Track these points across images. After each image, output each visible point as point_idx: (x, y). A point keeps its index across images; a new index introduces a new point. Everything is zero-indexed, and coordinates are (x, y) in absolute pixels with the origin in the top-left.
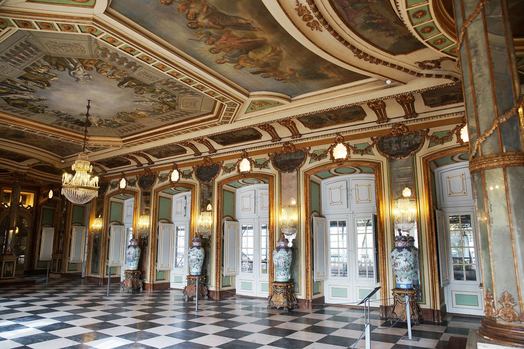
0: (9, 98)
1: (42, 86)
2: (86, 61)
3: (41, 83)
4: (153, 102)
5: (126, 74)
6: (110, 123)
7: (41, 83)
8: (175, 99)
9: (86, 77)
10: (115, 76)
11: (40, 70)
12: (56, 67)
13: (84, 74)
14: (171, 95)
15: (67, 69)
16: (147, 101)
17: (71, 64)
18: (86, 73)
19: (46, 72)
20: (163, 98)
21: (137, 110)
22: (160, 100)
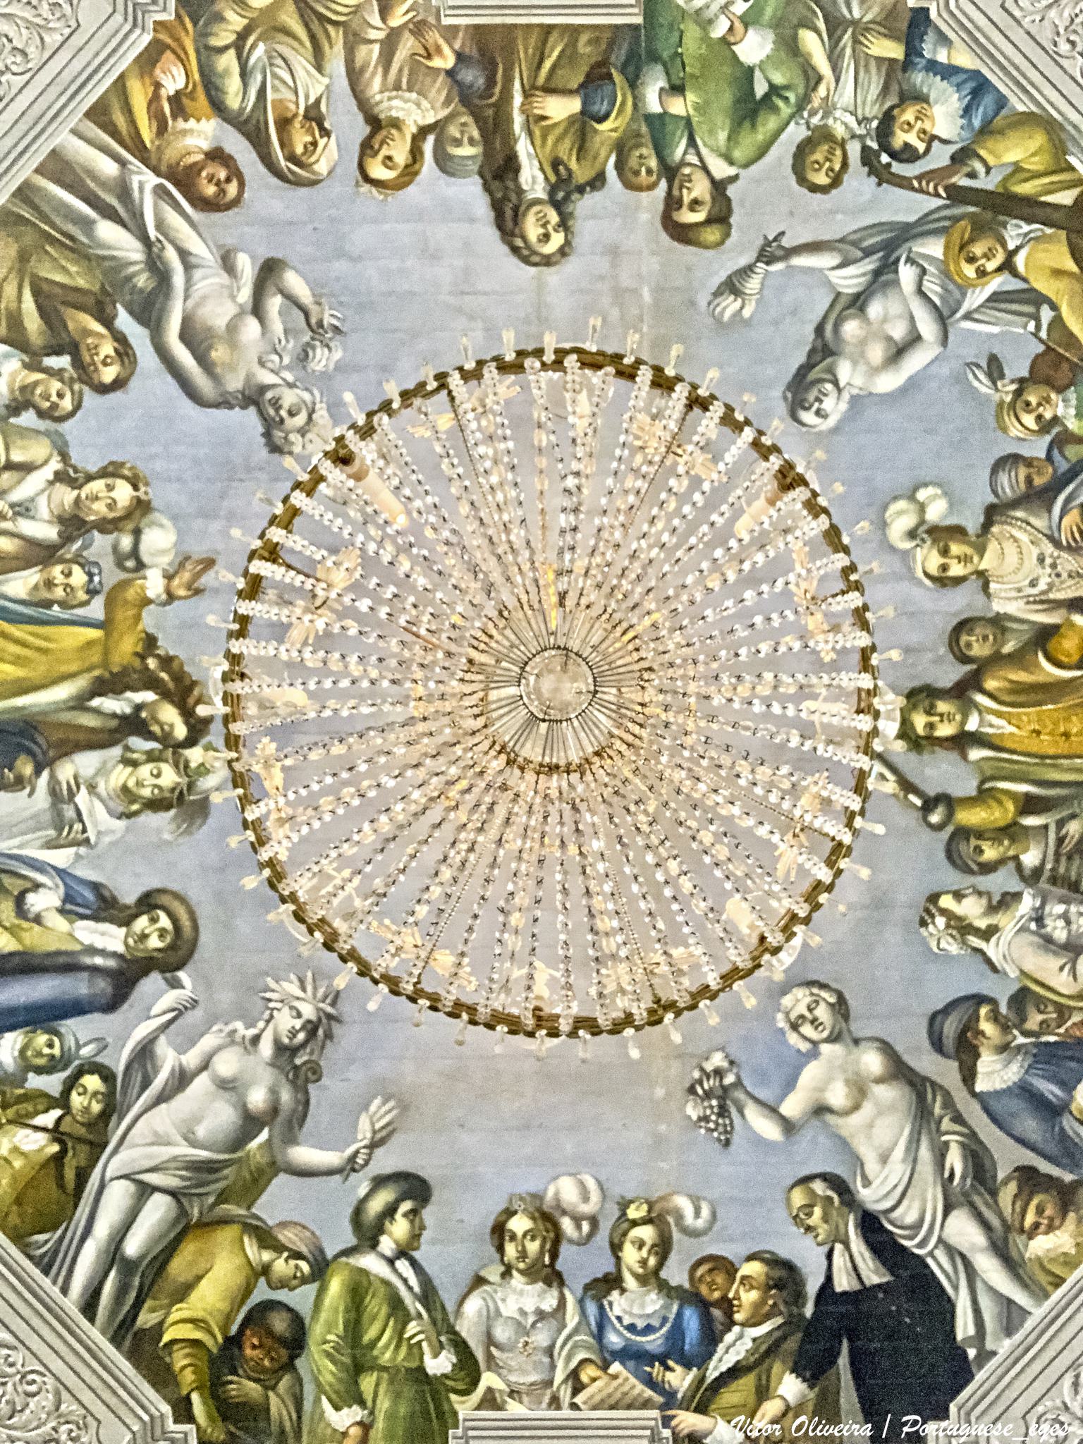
0: (113, 1254)
1: (169, 777)
2: (139, 97)
3: (135, 724)
4: (907, 274)
5: (418, 28)
6: (1024, 1090)
7: (135, 724)
8: (964, 59)
9: (274, 303)
10: (396, 124)
11: (23, 510)
12: (63, 362)
13: (245, 295)
14: (887, 25)
15: (124, 320)
16: (858, 303)
17: (108, 231)
18: (246, 266)
19: (67, 496)
20: (887, 121)
21: (942, 535)
22: (903, 183)
